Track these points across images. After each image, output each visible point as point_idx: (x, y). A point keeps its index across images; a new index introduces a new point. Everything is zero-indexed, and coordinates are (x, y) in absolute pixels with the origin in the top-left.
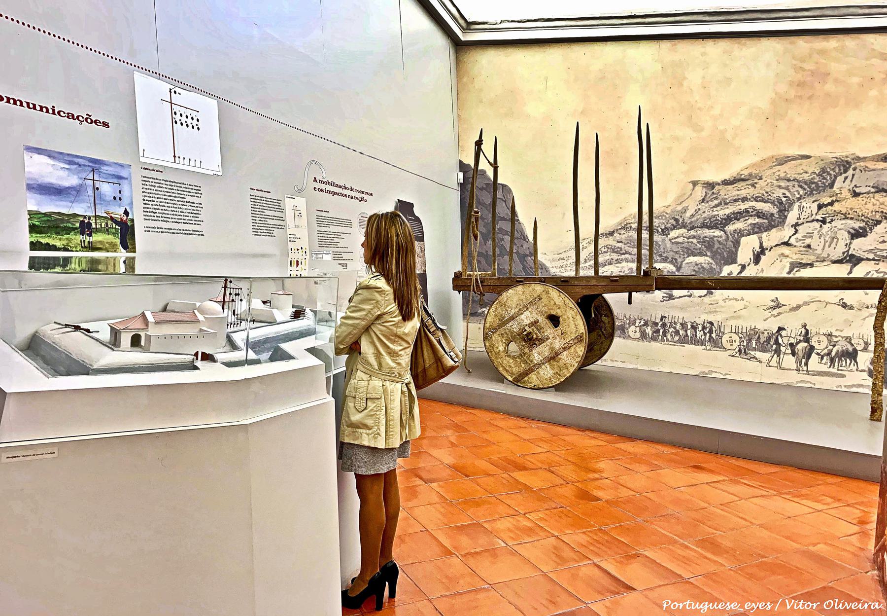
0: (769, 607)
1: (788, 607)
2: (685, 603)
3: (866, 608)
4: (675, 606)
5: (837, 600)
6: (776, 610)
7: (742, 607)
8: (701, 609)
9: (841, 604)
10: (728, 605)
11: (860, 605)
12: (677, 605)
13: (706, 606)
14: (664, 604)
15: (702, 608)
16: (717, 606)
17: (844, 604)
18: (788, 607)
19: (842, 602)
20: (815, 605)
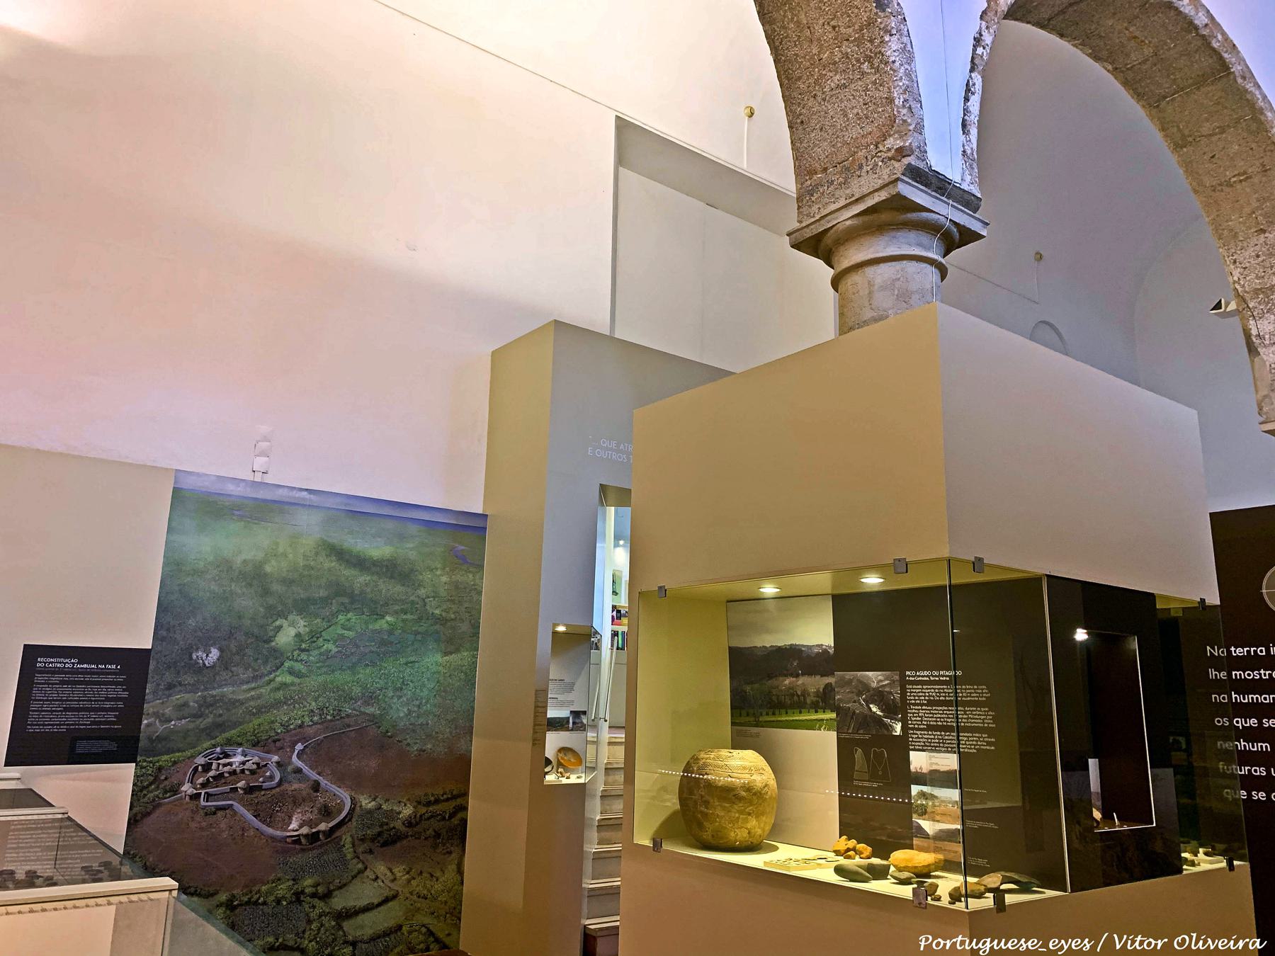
0: (1088, 946)
1: (1118, 947)
2: (1248, 940)
3: (1240, 948)
4: (938, 944)
5: (1195, 935)
6: (1098, 950)
7: (1045, 945)
8: (980, 949)
9: (1201, 942)
10: (1023, 944)
11: (1232, 942)
12: (942, 942)
13: (988, 944)
14: (921, 941)
15: (981, 947)
16: (1005, 945)
17: (1205, 942)
18: (1118, 947)
19: (1202, 938)
20: (1160, 943)
